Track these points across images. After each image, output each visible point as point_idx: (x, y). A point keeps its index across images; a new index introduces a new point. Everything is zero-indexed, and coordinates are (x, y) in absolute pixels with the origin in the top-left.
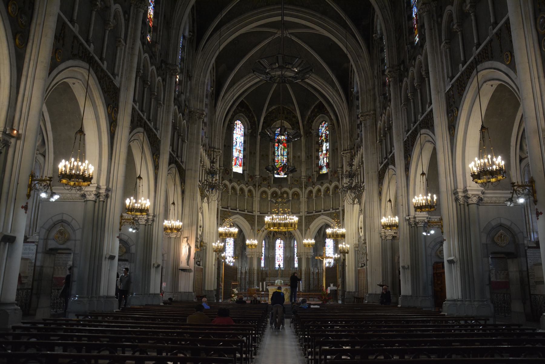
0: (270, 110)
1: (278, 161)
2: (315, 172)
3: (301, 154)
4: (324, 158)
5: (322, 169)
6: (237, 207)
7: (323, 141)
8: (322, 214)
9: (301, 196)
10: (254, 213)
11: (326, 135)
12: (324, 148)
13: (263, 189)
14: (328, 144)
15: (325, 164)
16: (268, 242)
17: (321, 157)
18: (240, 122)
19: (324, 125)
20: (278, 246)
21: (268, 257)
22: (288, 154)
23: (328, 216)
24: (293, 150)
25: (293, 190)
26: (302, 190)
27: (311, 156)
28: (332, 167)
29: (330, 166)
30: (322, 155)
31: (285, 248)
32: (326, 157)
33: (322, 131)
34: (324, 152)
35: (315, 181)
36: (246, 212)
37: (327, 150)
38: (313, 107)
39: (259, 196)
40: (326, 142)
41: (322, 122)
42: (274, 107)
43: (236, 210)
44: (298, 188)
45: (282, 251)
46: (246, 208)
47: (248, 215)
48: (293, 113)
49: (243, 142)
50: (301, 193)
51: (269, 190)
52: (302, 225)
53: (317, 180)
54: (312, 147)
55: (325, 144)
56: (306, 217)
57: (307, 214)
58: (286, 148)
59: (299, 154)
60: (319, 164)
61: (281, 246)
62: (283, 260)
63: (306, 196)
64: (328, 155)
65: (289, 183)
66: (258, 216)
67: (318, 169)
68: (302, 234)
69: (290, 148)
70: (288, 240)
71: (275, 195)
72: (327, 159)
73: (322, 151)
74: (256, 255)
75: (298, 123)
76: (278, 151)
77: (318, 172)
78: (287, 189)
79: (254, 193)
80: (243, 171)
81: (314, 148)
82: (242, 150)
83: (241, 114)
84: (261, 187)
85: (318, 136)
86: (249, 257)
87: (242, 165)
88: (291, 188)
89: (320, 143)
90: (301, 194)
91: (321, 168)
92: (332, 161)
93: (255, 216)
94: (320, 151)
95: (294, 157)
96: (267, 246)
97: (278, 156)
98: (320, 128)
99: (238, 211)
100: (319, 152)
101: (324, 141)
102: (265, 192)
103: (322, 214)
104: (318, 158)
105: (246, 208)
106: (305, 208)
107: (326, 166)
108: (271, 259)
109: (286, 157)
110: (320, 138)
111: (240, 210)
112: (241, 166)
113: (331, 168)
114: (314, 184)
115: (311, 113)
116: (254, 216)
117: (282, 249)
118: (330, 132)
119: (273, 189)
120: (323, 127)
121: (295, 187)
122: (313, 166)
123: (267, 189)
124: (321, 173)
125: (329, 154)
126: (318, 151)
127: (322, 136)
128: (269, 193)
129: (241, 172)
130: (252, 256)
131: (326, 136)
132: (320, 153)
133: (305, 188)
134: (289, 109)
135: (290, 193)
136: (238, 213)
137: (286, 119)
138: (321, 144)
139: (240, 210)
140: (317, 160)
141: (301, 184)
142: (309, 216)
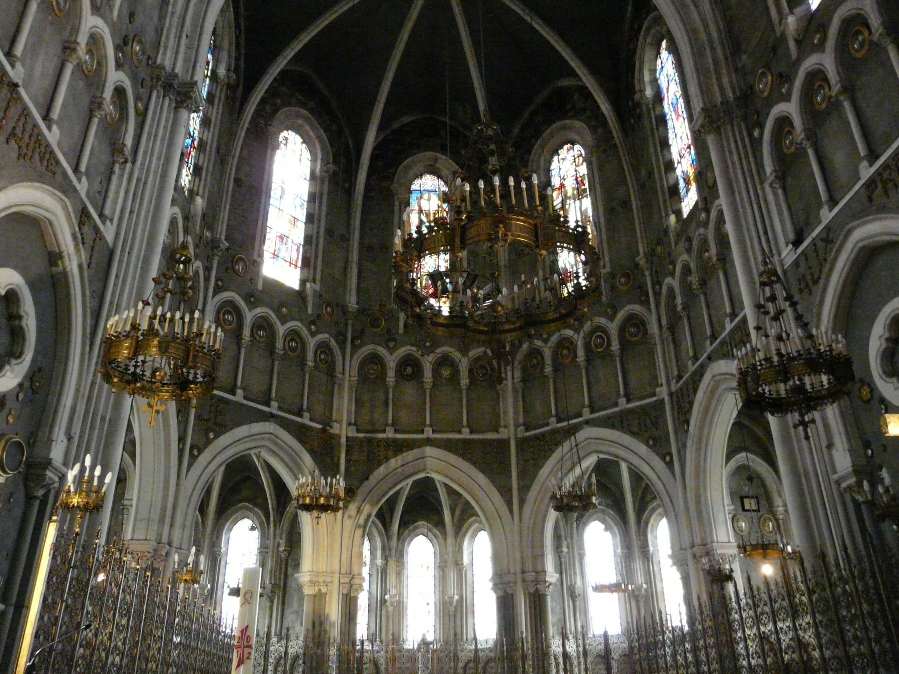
0: (396, 125)
2: (546, 290)
6: (273, 395)
8: (587, 422)
10: (335, 429)
13: (366, 350)
14: (587, 203)
18: (299, 139)
21: (383, 602)
23: (613, 427)
31: (442, 567)
36: (305, 420)
38: (526, 114)
39: (355, 372)
42: (407, 119)
43: (268, 405)
45: (431, 581)
46: (305, 407)
49: (306, 198)
52: (510, 472)
56: (522, 444)
57: (527, 430)
68: (510, 504)
70: (450, 540)
79: (339, 359)
80: (303, 282)
82: (303, 218)
84: (360, 347)
86: (308, 591)
87: (299, 264)
93: (339, 437)
96: (379, 561)
99: (274, 408)
102: (374, 359)
103: (587, 422)
106: (516, 413)
108: (390, 609)
111: (280, 409)
112: (296, 266)
113: (608, 266)
115: (522, 130)
119: (402, 351)
123: (381, 351)
128: (391, 361)
129: (296, 285)
130: (324, 590)
131: (579, 182)
136: (272, 416)
139: (280, 409)
142: (536, 438)
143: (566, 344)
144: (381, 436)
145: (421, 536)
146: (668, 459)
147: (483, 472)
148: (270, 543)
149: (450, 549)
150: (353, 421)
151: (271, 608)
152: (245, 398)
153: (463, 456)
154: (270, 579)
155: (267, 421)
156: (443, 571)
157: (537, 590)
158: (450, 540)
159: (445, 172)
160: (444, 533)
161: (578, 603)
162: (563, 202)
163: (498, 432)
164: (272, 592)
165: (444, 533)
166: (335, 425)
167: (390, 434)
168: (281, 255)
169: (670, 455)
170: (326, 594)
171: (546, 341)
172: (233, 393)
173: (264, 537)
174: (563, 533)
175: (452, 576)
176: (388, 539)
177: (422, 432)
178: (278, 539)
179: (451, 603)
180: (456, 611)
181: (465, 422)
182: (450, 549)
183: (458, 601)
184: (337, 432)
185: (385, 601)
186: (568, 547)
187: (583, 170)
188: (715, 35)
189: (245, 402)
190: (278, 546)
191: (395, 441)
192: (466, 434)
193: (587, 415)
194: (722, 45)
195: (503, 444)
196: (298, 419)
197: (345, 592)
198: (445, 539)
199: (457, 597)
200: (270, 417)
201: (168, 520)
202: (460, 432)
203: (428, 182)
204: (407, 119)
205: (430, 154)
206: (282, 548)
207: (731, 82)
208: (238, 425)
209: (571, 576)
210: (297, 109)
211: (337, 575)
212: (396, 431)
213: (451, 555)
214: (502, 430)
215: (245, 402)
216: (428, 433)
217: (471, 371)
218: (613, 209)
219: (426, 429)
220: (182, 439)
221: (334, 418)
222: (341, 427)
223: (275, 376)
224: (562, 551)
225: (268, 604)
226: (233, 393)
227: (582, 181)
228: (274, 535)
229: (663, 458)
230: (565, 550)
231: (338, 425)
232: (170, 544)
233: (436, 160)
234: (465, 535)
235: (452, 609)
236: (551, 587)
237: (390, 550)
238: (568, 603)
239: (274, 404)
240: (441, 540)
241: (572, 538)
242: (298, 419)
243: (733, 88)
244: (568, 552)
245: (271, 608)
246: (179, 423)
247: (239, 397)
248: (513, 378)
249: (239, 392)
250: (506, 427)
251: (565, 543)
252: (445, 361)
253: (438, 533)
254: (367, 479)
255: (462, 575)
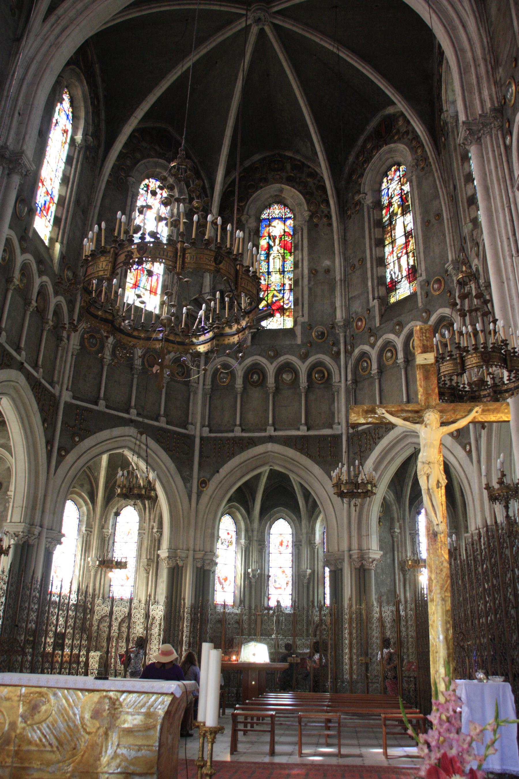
1: (268, 286)
2: (374, 299)
3: (334, 262)
4: (399, 258)
5: (396, 289)
6: (133, 404)
7: (393, 215)
9: (335, 378)
10: (191, 430)
11: (401, 197)
12: (399, 232)
14: (409, 218)
15: (405, 273)
16: (247, 531)
17: (391, 259)
19: (395, 174)
20: (278, 544)
22: (296, 265)
24: (310, 253)
25: (311, 360)
26: (336, 356)
27: (363, 261)
28: (426, 269)
29: (422, 269)
30: (393, 251)
31: (297, 545)
32: (407, 253)
33: (390, 191)
34: (401, 241)
35: (378, 325)
36: (162, 423)
37: (407, 235)
38: (360, 142)
39: (209, 381)
40: (403, 214)
41: (390, 169)
42: (257, 157)
43: (128, 412)
44: (324, 353)
45: (290, 557)
46: (162, 412)
47: (169, 431)
48: (309, 167)
50: (336, 367)
51: (240, 363)
53: (380, 321)
54: (364, 237)
55: (399, 222)
58: (291, 253)
59: (327, 263)
60: (385, 277)
61: (285, 544)
62: (290, 584)
63: (350, 377)
64: (411, 247)
65: (299, 341)
66: (202, 438)
67: (382, 291)
69: (302, 250)
70: (304, 522)
71: (255, 377)
72: (408, 257)
73: (393, 242)
74: (190, 559)
75: (323, 189)
76: (268, 263)
77: (384, 301)
78: (294, 360)
81: (370, 239)
83: (161, 161)
85: (378, 205)
87: (159, 291)
88: (304, 358)
89: (387, 223)
90: (337, 372)
91: (393, 286)
92: (424, 252)
93: (194, 437)
94: (387, 242)
95: (313, 272)
97: (269, 273)
98: (384, 186)
99: (133, 414)
100: (384, 246)
101: (396, 214)
104: (382, 262)
105: (162, 412)
107: (408, 277)
109: (291, 276)
110: (384, 212)
111: (139, 415)
112: (155, 294)
113: (424, 274)
114: (373, 332)
115: (357, 157)
116: (191, 438)
117: (290, 549)
118: (415, 184)
119: (249, 361)
120: (392, 180)
121: (317, 353)
122: (370, 284)
124: (392, 300)
125: (416, 243)
126: (381, 244)
127: (390, 204)
130: (180, 564)
131: (403, 199)
132: (388, 249)
133: (346, 351)
134: (298, 157)
135: (303, 368)
136: (132, 421)
137: (290, 181)
138: (391, 223)
139: (139, 415)
140: (380, 269)
141: (336, 343)
143: (389, 346)
144: (231, 435)
145: (281, 520)
146: (468, 448)
147: (318, 463)
148: (146, 525)
149: (304, 531)
150: (207, 423)
151: (148, 578)
152: (107, 407)
153: (301, 451)
154: (147, 555)
155: (128, 425)
156: (299, 550)
157: (362, 565)
158: (304, 522)
159: (289, 201)
160: (299, 517)
161: (408, 577)
162: (390, 219)
163: (332, 428)
164: (148, 565)
165: (299, 517)
166: (190, 427)
167: (238, 433)
168: (142, 285)
169: (470, 444)
170: (183, 567)
171: (373, 346)
172: (96, 404)
173: (142, 520)
174: (396, 516)
175: (305, 552)
176: (251, 522)
177: (265, 430)
178: (152, 523)
179: (304, 576)
180: (309, 583)
181: (303, 421)
182: (304, 531)
183: (310, 574)
184: (192, 433)
185: (249, 574)
186: (400, 528)
187: (407, 188)
188: (479, 52)
189: (108, 411)
190: (153, 528)
191: (241, 439)
192: (303, 431)
193: (133, 414)
194: (485, 60)
195: (337, 438)
196: (156, 423)
197: (199, 565)
198: (300, 522)
199: (309, 571)
200: (130, 422)
201: (39, 507)
202: (298, 429)
203: (276, 210)
204: (257, 157)
205: (277, 186)
206: (155, 530)
207: (490, 95)
208: (101, 430)
209: (402, 553)
210: (156, 159)
211: (191, 553)
212: (243, 430)
213: (304, 536)
214: (335, 426)
215: (108, 411)
216: (271, 431)
217: (309, 376)
218: (429, 222)
219: (268, 428)
220: (49, 442)
221: (190, 421)
222: (195, 428)
223: (134, 388)
224: (395, 532)
225: (145, 575)
226: (96, 404)
227: (406, 198)
228: (150, 519)
229: (464, 448)
230: (397, 530)
231: (193, 427)
232: (41, 526)
233: (281, 191)
234: (317, 518)
235: (306, 581)
236: (375, 562)
237: (252, 531)
238: (399, 576)
239: (133, 411)
240: (297, 522)
241: (404, 519)
242: (156, 423)
243: (491, 99)
244: (400, 533)
245: (148, 578)
246: (46, 430)
247: (101, 406)
248: (346, 380)
249: (102, 403)
250: (339, 424)
251: (397, 525)
252: (288, 367)
253: (294, 517)
254: (218, 472)
255: (314, 552)
